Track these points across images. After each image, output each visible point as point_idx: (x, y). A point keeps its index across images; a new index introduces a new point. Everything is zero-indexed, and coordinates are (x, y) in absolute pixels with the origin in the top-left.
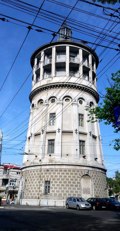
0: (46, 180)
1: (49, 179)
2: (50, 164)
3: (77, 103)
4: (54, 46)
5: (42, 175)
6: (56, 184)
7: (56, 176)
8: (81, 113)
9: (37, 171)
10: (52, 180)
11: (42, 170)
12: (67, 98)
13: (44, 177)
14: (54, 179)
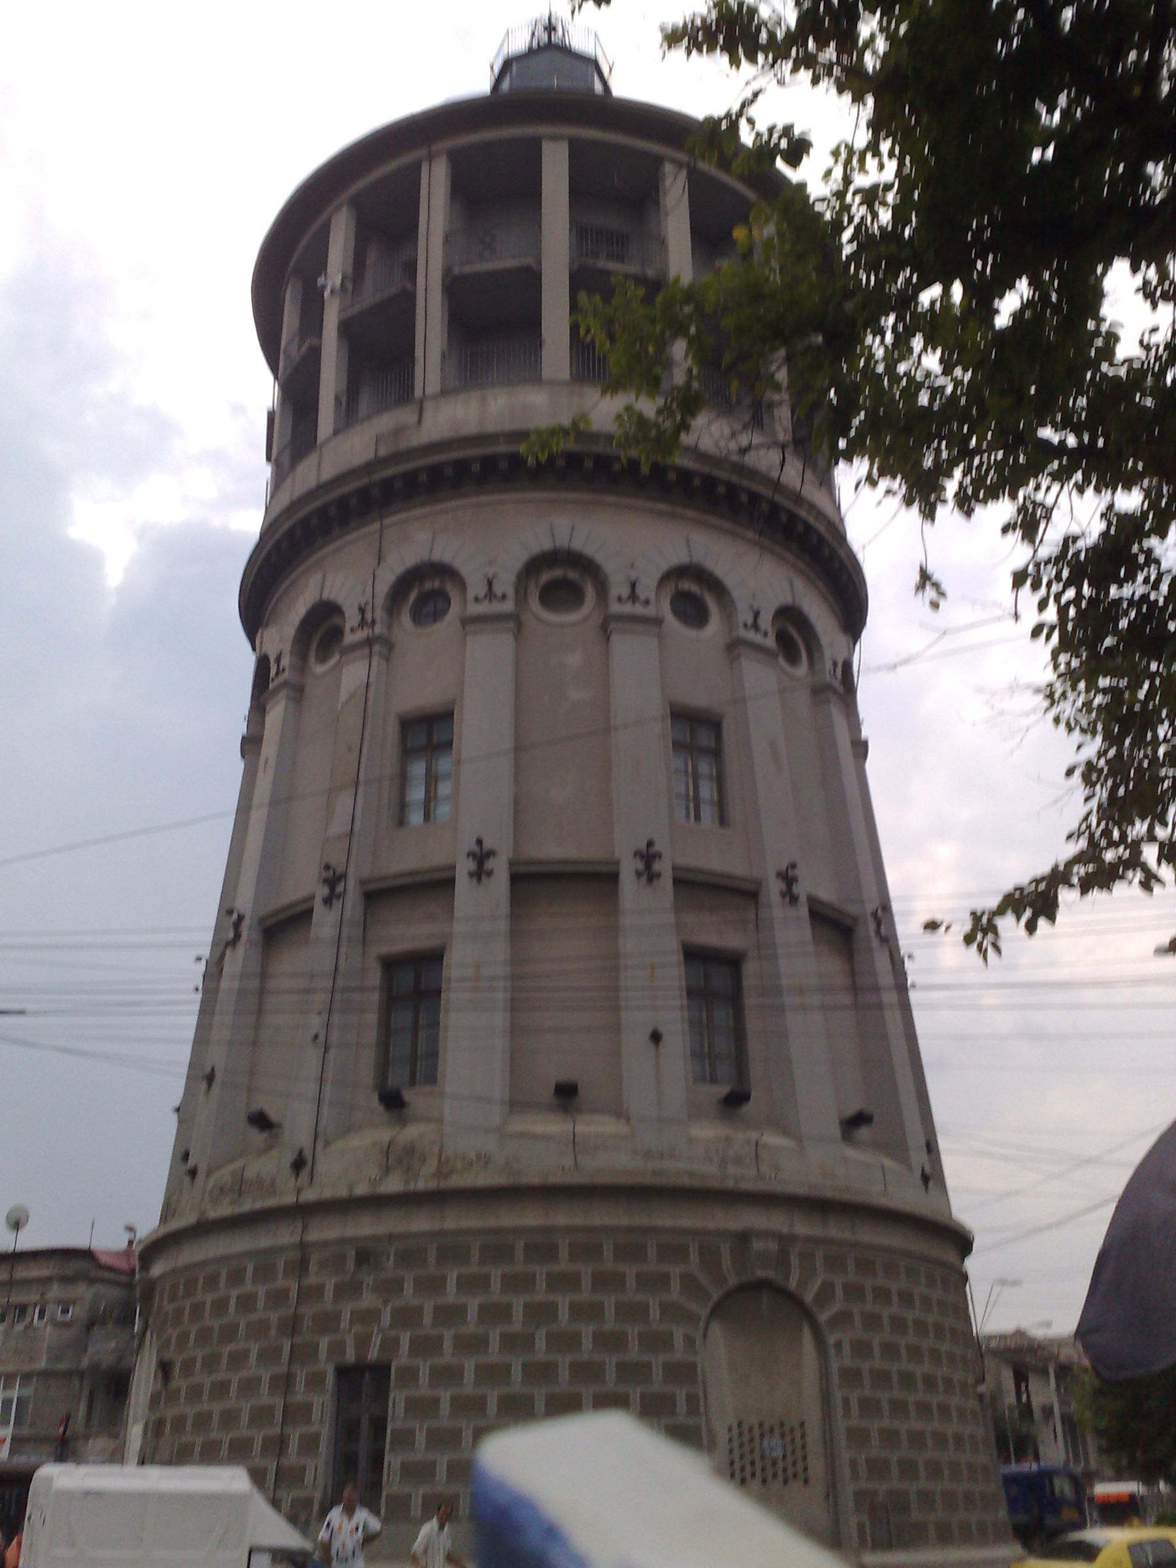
0: (350, 1356)
1: (376, 1341)
2: (393, 1185)
3: (650, 611)
4: (434, 148)
5: (309, 1311)
6: (446, 1396)
7: (450, 1314)
8: (698, 697)
9: (264, 1272)
10: (401, 1359)
11: (315, 1258)
12: (557, 573)
13: (328, 1322)
14: (426, 1346)
